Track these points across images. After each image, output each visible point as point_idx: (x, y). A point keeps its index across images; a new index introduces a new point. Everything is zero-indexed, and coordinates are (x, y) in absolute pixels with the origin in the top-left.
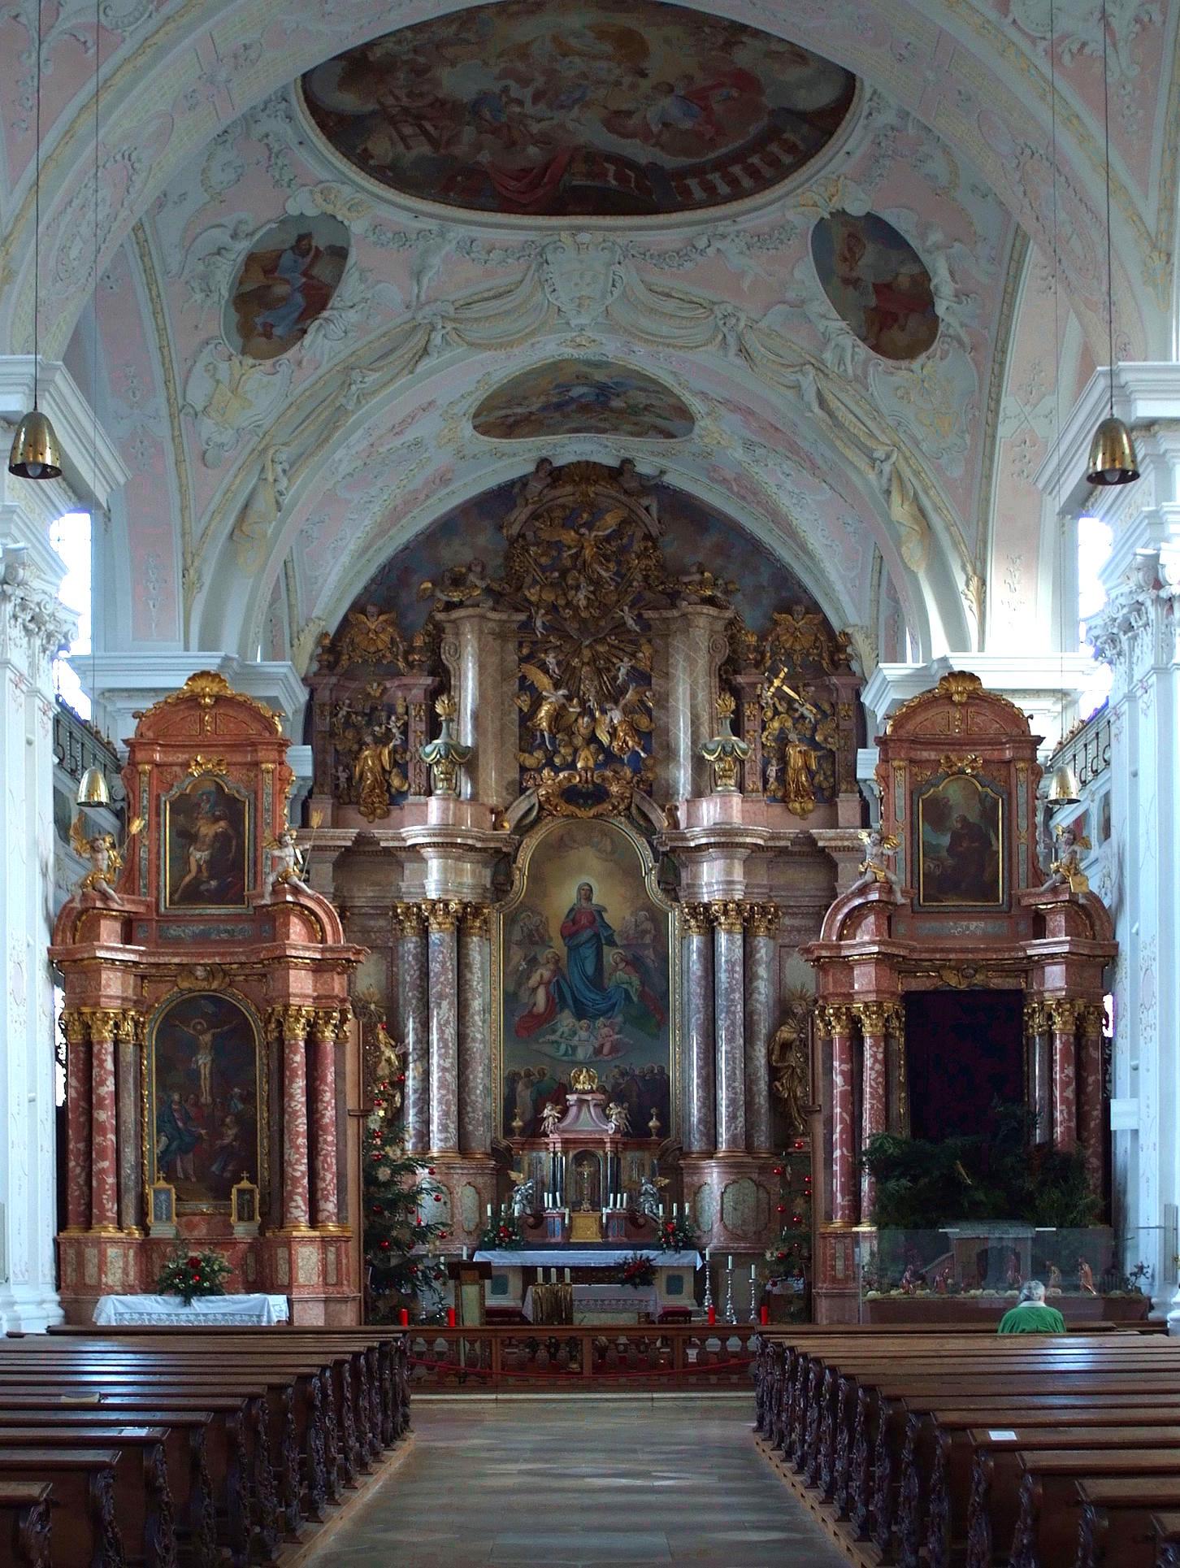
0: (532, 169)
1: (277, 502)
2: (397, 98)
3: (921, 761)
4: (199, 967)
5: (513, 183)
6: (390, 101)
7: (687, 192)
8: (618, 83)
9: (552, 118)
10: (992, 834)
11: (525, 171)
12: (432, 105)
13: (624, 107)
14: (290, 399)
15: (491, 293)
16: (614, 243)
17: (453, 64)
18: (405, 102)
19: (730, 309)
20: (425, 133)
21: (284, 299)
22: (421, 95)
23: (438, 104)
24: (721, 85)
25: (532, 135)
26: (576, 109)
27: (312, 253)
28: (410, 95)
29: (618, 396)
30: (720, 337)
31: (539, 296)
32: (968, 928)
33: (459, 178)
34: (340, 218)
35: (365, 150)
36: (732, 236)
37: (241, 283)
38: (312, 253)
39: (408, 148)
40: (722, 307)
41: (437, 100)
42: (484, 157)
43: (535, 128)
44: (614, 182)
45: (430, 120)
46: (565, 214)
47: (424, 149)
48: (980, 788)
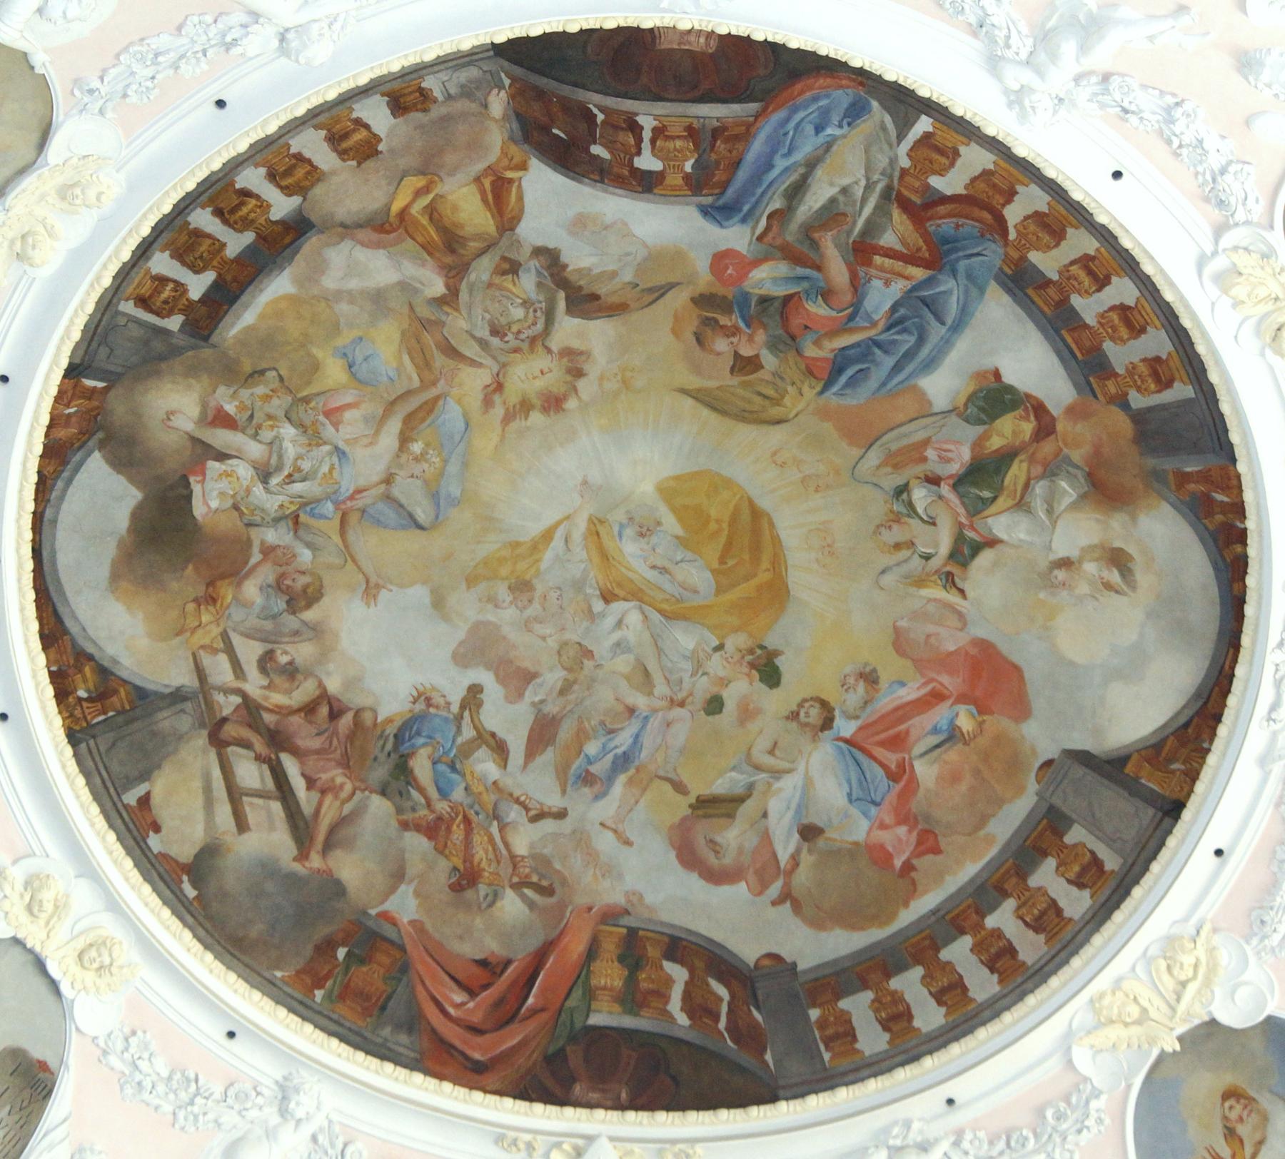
0: (508, 962)
5: (459, 997)
6: (220, 670)
7: (844, 1034)
8: (714, 705)
9: (561, 815)
11: (490, 967)
12: (309, 709)
13: (721, 786)
17: (371, 591)
18: (254, 684)
22: (292, 672)
23: (324, 710)
24: (936, 697)
25: (513, 857)
26: (618, 788)
28: (266, 661)
33: (341, 953)
35: (145, 801)
36: (945, 1146)
39: (242, 825)
41: (324, 696)
43: (524, 839)
44: (683, 1019)
45: (295, 752)
46: (561, 1102)
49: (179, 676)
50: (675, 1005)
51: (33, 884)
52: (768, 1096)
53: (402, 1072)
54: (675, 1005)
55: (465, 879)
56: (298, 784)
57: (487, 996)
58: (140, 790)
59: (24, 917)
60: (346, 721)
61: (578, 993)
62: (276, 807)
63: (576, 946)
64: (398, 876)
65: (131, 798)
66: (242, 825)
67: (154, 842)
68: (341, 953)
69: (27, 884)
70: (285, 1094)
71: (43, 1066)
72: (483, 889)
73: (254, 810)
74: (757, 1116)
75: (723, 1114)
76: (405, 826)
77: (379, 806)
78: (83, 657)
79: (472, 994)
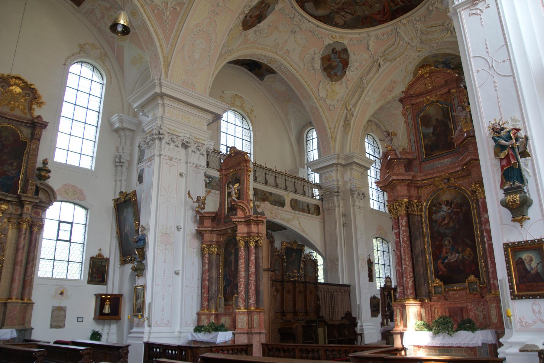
1: (352, 114)
2: (333, 6)
3: (417, 103)
4: (228, 230)
5: (379, 16)
6: (333, 8)
10: (448, 122)
11: (380, 11)
12: (343, 4)
14: (349, 90)
15: (390, 46)
16: (412, 20)
18: (336, 6)
19: (448, 22)
20: (347, 12)
21: (336, 66)
22: (339, 3)
23: (345, 4)
27: (338, 52)
28: (336, 4)
29: (450, 64)
30: (449, 31)
31: (401, 42)
32: (444, 162)
33: (364, 20)
34: (339, 41)
35: (335, 23)
36: (437, 2)
37: (323, 66)
38: (338, 52)
39: (346, 18)
40: (446, 23)
42: (367, 12)
44: (402, 4)
45: (345, 9)
46: (396, 18)
47: (349, 17)
48: (441, 105)
49: (329, 11)
50: (400, 3)
51: (332, 36)
52: (416, 6)
53: (378, 26)
54: (400, 3)
55: (371, 6)
56: (348, 11)
57: (382, 13)
58: (334, 22)
59: (334, 39)
60: (347, 3)
61: (390, 8)
62: (348, 14)
63: (386, 4)
64: (364, 11)
65: (334, 23)
66: (346, 18)
67: (339, 25)
68: (364, 20)
69: (331, 37)
70: (369, 35)
71: (345, 49)
72: (373, 6)
73: (346, 16)
74: (416, 9)
75: (413, 10)
76: (361, 6)
77: (357, 7)
78: (320, 17)
79: (380, 15)
